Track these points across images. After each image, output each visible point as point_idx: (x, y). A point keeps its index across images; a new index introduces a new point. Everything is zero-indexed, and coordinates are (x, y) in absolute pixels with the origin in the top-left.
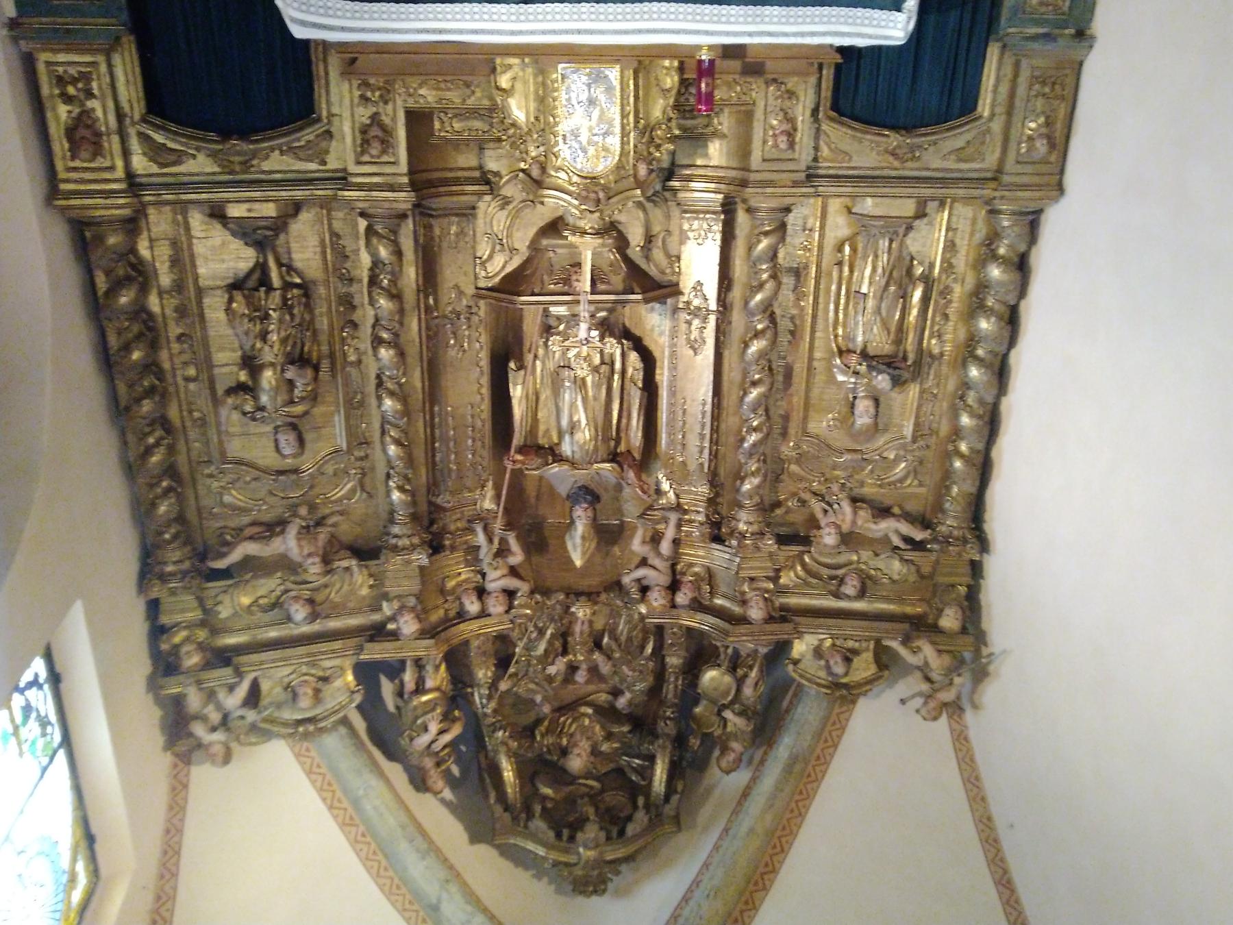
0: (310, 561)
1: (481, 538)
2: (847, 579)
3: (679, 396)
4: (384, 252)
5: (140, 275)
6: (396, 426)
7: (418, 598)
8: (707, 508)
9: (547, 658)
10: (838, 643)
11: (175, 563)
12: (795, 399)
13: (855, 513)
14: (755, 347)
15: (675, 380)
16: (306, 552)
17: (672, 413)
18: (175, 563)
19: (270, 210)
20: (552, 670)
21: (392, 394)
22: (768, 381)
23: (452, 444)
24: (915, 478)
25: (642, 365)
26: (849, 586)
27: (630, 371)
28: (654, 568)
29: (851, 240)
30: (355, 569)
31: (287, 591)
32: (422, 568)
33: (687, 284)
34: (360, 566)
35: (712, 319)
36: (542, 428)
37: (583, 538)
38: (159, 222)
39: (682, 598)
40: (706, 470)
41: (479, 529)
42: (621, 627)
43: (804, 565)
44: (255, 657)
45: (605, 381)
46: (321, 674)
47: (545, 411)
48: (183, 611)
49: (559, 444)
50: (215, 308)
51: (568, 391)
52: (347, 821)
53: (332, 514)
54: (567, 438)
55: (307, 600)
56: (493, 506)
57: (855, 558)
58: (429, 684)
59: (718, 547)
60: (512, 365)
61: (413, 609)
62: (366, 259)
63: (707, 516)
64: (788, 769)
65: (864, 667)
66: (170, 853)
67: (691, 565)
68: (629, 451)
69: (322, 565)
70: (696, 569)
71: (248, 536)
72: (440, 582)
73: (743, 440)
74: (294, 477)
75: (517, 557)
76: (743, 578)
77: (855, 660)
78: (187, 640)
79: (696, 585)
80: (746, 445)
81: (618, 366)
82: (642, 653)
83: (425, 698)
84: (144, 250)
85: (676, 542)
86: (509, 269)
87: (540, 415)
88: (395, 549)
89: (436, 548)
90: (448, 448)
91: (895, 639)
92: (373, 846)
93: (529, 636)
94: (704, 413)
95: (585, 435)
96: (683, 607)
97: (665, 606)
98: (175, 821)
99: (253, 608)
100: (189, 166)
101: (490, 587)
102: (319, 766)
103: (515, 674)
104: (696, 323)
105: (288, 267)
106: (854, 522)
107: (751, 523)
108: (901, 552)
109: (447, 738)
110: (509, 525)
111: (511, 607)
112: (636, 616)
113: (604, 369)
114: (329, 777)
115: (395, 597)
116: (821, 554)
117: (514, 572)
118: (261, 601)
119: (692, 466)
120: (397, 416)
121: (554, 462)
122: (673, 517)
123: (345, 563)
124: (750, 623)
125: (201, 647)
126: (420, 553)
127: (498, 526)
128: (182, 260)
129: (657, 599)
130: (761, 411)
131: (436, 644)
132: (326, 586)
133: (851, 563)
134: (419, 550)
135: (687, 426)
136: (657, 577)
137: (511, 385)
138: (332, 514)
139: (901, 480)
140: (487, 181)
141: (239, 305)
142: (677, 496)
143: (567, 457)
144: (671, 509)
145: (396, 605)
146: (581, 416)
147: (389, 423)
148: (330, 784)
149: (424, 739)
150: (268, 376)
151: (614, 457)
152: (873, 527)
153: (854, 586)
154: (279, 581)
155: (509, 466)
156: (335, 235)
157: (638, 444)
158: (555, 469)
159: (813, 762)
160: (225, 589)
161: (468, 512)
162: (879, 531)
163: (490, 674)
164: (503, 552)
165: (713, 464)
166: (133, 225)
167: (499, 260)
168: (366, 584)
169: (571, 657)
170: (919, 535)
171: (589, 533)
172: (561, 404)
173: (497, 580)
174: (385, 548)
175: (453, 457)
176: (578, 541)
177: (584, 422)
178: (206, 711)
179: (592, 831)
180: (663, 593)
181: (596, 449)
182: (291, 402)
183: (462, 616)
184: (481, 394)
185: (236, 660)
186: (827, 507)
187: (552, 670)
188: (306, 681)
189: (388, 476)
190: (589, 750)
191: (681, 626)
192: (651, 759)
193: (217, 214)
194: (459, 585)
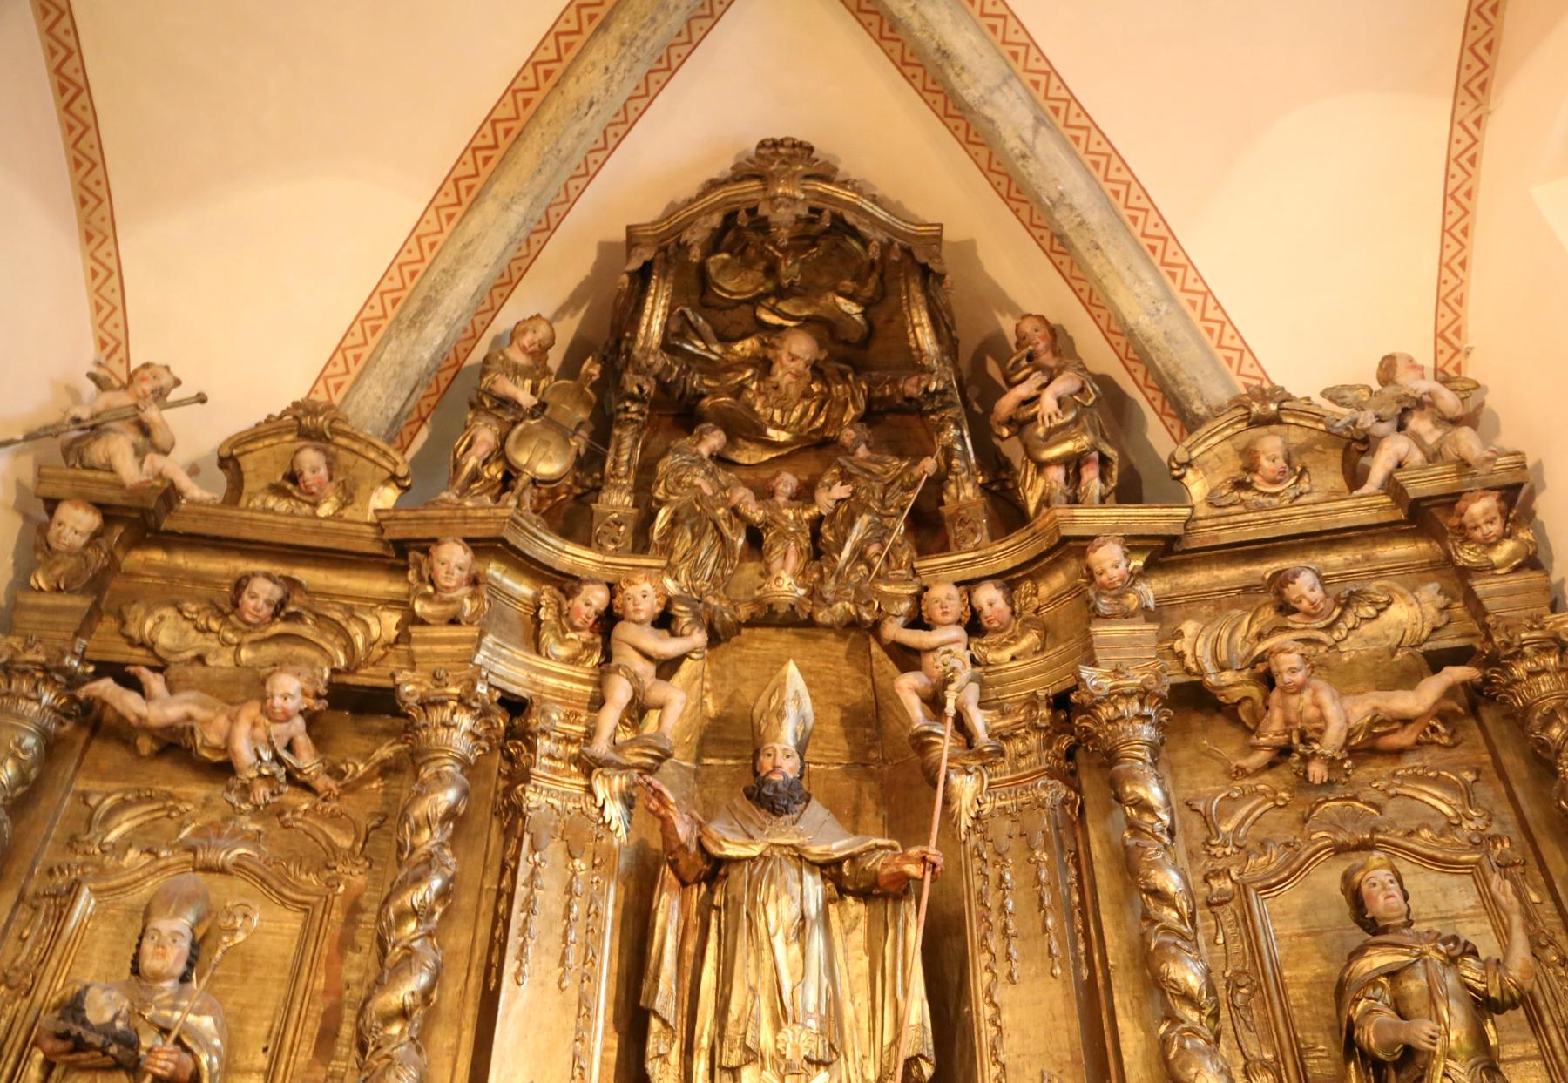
0: (1299, 677)
1: (979, 721)
2: (266, 611)
3: (573, 996)
6: (1168, 930)
7: (1095, 608)
8: (533, 763)
9: (849, 511)
10: (306, 509)
11: (1544, 671)
12: (320, 984)
13: (228, 739)
15: (577, 1032)
16: (1306, 696)
17: (589, 959)
18: (1544, 671)
20: (841, 491)
21: (1188, 998)
22: (372, 1019)
23: (1047, 902)
24: (93, 810)
25: (649, 1066)
26: (263, 596)
27: (675, 1057)
28: (647, 656)
30: (1209, 666)
31: (1329, 628)
32: (1094, 664)
34: (1202, 673)
36: (859, 937)
37: (781, 715)
39: (596, 597)
40: (527, 838)
41: (982, 736)
42: (712, 560)
43: (349, 646)
44: (1367, 517)
45: (731, 1030)
46: (1244, 495)
47: (854, 972)
48: (1510, 592)
49: (828, 901)
51: (811, 1008)
52: (1180, 272)
53: (1259, 771)
54: (812, 909)
55: (1295, 611)
56: (956, 780)
57: (245, 654)
58: (1057, 474)
59: (516, 690)
60: (928, 1070)
61: (1103, 589)
63: (532, 748)
64: (429, 304)
65: (261, 467)
66: (1457, 231)
67: (572, 660)
68: (684, 884)
69: (1274, 669)
70: (563, 651)
71: (1410, 727)
72: (1048, 645)
73: (443, 894)
74: (1342, 837)
75: (908, 688)
76: (470, 624)
77: (279, 478)
78: (1491, 545)
79: (565, 620)
80: (436, 883)
82: (676, 513)
83: (1068, 447)
87: (865, 962)
88: (1143, 695)
90: (1054, 891)
91: (191, 502)
92: (1137, 231)
93: (883, 547)
94: (521, 954)
95: (779, 913)
96: (594, 581)
97: (629, 582)
98: (1453, 281)
99: (1385, 599)
101: (958, 633)
102: (1229, 360)
103: (907, 489)
106: (233, 720)
107: (444, 725)
108: (152, 662)
109: (1023, 391)
110: (922, 743)
111: (918, 598)
112: (683, 575)
113: (733, 1057)
114: (1212, 343)
115: (1133, 615)
116: (312, 665)
118: (1372, 611)
119: (554, 850)
120: (1173, 950)
121: (838, 863)
122: (601, 747)
123: (1228, 677)
124: (468, 540)
125: (1464, 533)
126: (1097, 687)
127: (945, 742)
129: (643, 597)
130: (395, 953)
131: (1057, 528)
132: (1260, 636)
133: (255, 644)
134: (1100, 694)
135: (560, 931)
136: (637, 636)
137: (928, 1024)
138: (1259, 771)
139: (124, 805)
142: (589, 790)
143: (812, 872)
144: (605, 764)
145: (1132, 600)
146: (786, 954)
147: (1183, 936)
148: (1210, 331)
151: (715, 869)
152: (199, 713)
153: (254, 596)
154: (1343, 647)
155: (932, 851)
157: (665, 896)
158: (838, 845)
159: (385, 323)
160: (1438, 635)
161: (1004, 770)
162: (187, 701)
163: (952, 489)
165: (511, 851)
168: (1187, 638)
169: (806, 516)
170: (106, 687)
171: (769, 724)
172: (825, 981)
174: (1162, 699)
175: (1043, 875)
176: (791, 710)
177: (778, 942)
178: (1438, 433)
179: (783, 217)
180: (630, 606)
181: (753, 886)
182: (1393, 974)
183: (1008, 580)
184: (992, 1003)
185: (1401, 515)
186: (285, 755)
187: (841, 491)
188: (1274, 482)
190: (776, 367)
191: (601, 549)
192: (666, 346)
194: (1015, 638)
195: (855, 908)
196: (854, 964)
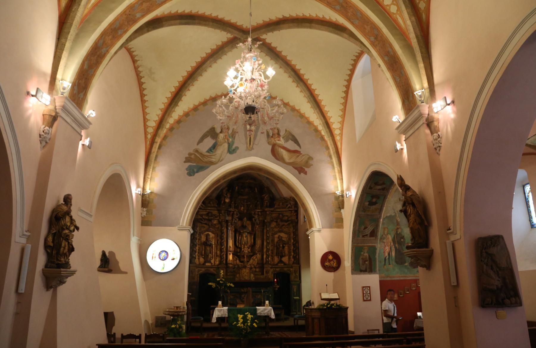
1: (258, 222)
4: (267, 260)
5: (294, 257)
14: (223, 247)
19: (279, 264)
20: (249, 203)
29: (211, 260)
33: (231, 255)
35: (228, 250)
38: (291, 262)
39: (232, 212)
41: (258, 223)
45: (242, 242)
50: (287, 252)
58: (265, 203)
62: (270, 259)
75: (253, 219)
81: (239, 244)
84: (293, 260)
85: (232, 220)
86: (253, 257)
89: (264, 221)
100: (287, 269)
104: (230, 250)
105: (278, 257)
109: (264, 195)
117: (254, 217)
119: (230, 231)
122: (233, 224)
127: (256, 224)
128: (289, 258)
129: (235, 213)
136: (235, 216)
140: (255, 268)
141: (284, 254)
146: (245, 238)
149: (267, 196)
150: (281, 246)
156: (273, 261)
164: (255, 220)
166: (294, 263)
167: (254, 258)
170: (201, 221)
173: (256, 217)
183: (261, 212)
189: (269, 232)
193: (285, 264)
195: (249, 234)
196: (249, 238)
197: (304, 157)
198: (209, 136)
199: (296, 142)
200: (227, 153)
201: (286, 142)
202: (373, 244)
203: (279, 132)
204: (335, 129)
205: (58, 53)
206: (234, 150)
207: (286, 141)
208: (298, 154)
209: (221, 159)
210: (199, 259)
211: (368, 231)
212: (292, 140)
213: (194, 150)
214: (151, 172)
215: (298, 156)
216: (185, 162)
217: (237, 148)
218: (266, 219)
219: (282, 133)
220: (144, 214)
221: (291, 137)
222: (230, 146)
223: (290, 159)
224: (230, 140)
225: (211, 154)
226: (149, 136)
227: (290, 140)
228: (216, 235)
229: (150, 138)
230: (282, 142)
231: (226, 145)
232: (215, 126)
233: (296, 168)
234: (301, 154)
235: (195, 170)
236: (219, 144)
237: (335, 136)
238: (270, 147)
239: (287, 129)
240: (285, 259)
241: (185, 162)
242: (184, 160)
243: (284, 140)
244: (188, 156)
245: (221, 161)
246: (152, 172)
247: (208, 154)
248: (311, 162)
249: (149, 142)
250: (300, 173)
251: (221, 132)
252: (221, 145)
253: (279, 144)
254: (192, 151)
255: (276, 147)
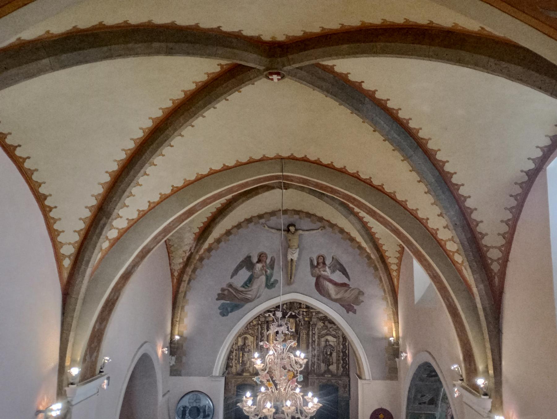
4: (313, 368)
19: (326, 376)
101: (302, 316)
166: (342, 375)
183: (306, 312)
193: (333, 375)
197: (354, 291)
198: (245, 267)
199: (344, 272)
200: (265, 288)
201: (333, 273)
202: (433, 413)
203: (325, 259)
204: (391, 264)
205: (65, 335)
206: (272, 284)
207: (333, 272)
208: (346, 288)
209: (258, 296)
210: (236, 366)
211: (427, 399)
212: (340, 271)
213: (227, 284)
214: (179, 311)
215: (346, 291)
216: (217, 299)
217: (276, 281)
218: (311, 320)
219: (328, 262)
220: (173, 363)
221: (338, 266)
222: (268, 278)
223: (337, 294)
224: (269, 271)
225: (247, 290)
226: (176, 274)
227: (338, 271)
228: (255, 337)
229: (178, 275)
230: (327, 272)
231: (263, 278)
232: (251, 254)
233: (343, 306)
234: (350, 288)
235: (229, 309)
236: (255, 276)
237: (391, 271)
238: (315, 279)
239: (334, 257)
240: (333, 368)
241: (217, 299)
242: (217, 297)
243: (330, 270)
244: (220, 292)
245: (258, 297)
246: (181, 312)
247: (243, 289)
248: (361, 298)
249: (177, 279)
250: (348, 312)
251: (258, 262)
252: (258, 278)
253: (324, 275)
254: (225, 286)
255: (321, 280)
